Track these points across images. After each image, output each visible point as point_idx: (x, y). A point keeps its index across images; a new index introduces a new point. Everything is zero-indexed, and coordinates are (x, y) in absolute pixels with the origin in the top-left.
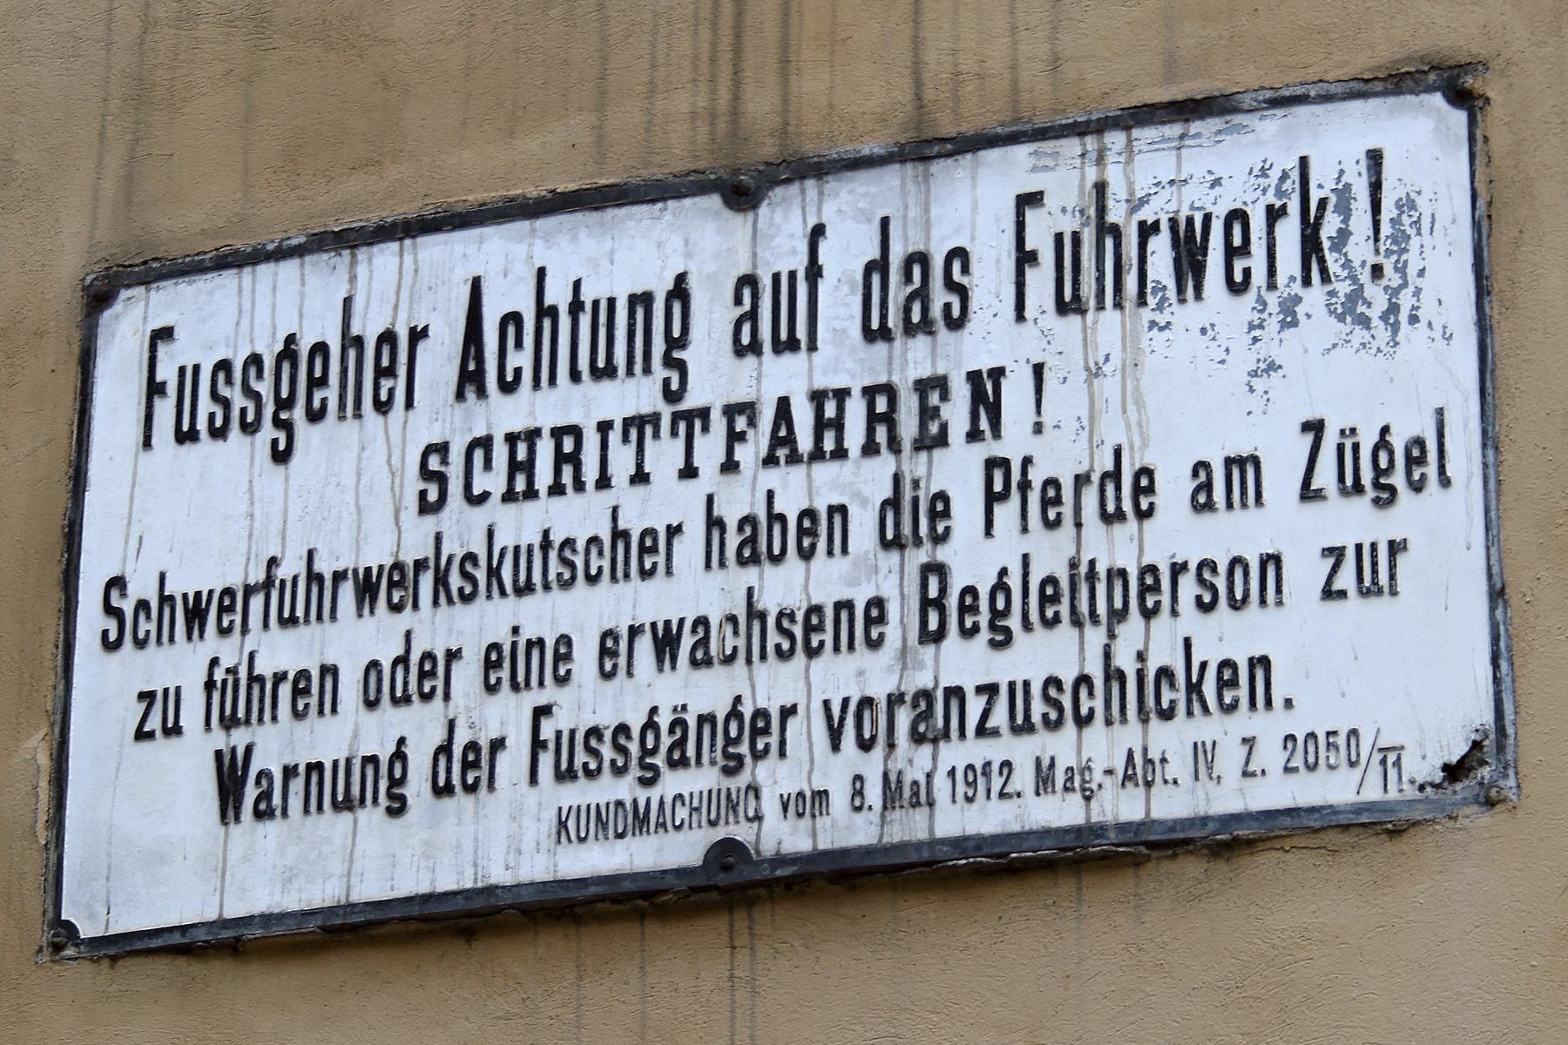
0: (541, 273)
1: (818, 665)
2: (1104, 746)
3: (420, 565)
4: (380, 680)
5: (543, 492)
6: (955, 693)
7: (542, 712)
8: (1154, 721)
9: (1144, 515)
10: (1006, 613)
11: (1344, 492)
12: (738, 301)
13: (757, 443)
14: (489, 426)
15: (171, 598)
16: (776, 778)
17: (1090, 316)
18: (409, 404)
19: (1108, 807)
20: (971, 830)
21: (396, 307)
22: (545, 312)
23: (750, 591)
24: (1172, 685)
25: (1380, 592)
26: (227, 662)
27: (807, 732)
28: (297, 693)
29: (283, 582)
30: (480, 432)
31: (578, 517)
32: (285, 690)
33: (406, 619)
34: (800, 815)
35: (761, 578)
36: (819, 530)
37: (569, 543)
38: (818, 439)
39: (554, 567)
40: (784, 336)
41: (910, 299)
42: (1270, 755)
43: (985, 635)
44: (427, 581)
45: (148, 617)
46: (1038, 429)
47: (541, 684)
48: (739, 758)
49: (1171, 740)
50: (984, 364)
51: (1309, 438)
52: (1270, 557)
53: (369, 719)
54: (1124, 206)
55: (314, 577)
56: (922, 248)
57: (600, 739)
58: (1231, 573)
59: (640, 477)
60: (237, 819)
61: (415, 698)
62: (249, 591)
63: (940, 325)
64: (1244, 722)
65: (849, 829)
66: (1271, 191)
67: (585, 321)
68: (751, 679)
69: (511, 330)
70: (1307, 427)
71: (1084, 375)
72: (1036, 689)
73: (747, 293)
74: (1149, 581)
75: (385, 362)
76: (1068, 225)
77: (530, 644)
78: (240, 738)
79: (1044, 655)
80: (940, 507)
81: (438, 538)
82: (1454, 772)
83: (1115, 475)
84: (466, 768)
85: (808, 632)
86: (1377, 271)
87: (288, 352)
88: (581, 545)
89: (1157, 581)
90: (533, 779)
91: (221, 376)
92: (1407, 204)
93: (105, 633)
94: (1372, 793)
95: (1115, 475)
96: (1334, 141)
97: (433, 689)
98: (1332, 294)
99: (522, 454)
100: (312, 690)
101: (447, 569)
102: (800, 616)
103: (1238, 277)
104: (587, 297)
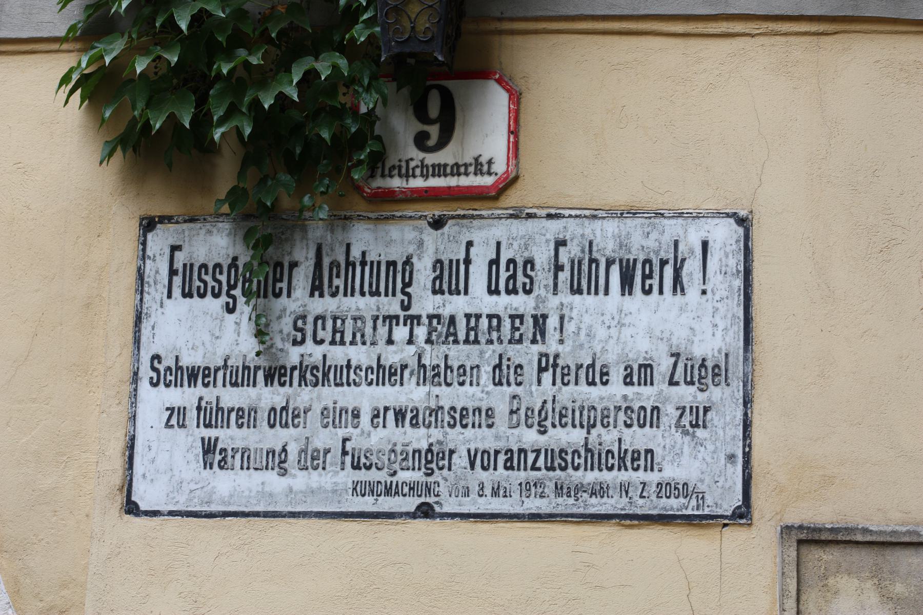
0: (348, 246)
3: (294, 368)
10: (546, 419)
12: (434, 271)
15: (181, 368)
22: (348, 263)
24: (613, 457)
28: (239, 417)
32: (233, 416)
37: (359, 367)
39: (352, 376)
40: (453, 287)
43: (536, 427)
44: (296, 373)
45: (171, 375)
62: (217, 370)
64: (641, 475)
67: (367, 269)
78: (212, 433)
83: (593, 365)
84: (313, 459)
85: (461, 417)
93: (151, 378)
95: (593, 365)
100: (245, 417)
103: (647, 287)
104: (368, 259)
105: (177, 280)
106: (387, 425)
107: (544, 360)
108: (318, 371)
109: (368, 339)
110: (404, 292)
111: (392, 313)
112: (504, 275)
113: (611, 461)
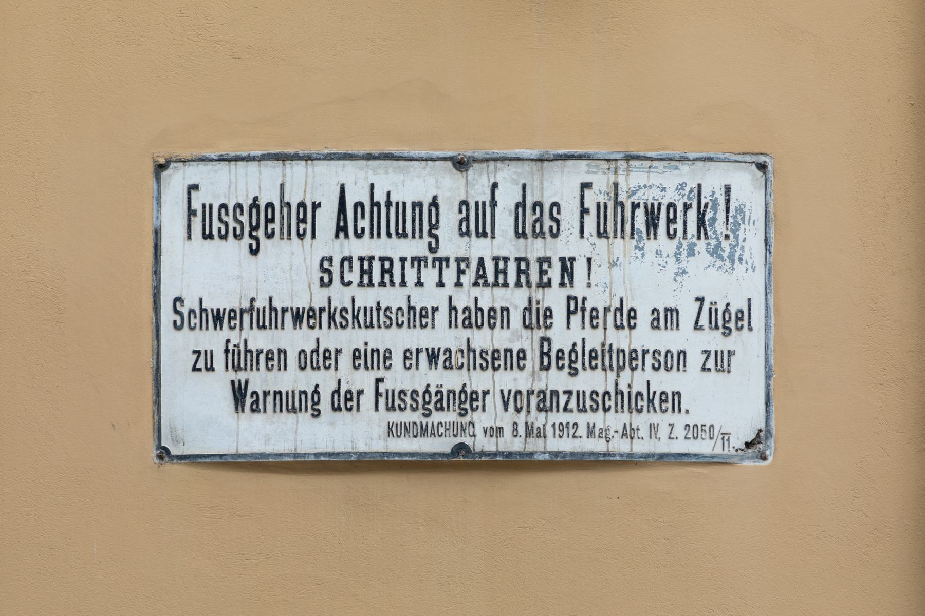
0: (372, 186)
1: (497, 374)
2: (615, 421)
3: (321, 310)
4: (306, 358)
5: (376, 285)
6: (555, 393)
7: (379, 380)
8: (634, 412)
9: (632, 328)
10: (575, 362)
11: (711, 328)
12: (460, 212)
13: (470, 276)
14: (350, 251)
15: (206, 310)
16: (482, 420)
17: (611, 240)
18: (313, 236)
19: (616, 445)
20: (561, 449)
21: (305, 191)
22: (374, 204)
23: (468, 339)
24: (642, 399)
25: (724, 371)
26: (234, 341)
27: (494, 402)
28: (268, 359)
29: (258, 309)
30: (347, 254)
31: (393, 298)
32: (262, 357)
33: (316, 333)
34: (491, 436)
35: (473, 334)
36: (496, 317)
37: (387, 309)
38: (496, 277)
39: (383, 318)
40: (481, 230)
41: (536, 221)
42: (679, 431)
43: (567, 370)
44: (325, 316)
46: (589, 285)
47: (379, 368)
48: (466, 410)
49: (641, 421)
50: (567, 255)
51: (699, 303)
52: (682, 351)
53: (302, 374)
54: (625, 195)
55: (272, 308)
56: (540, 200)
57: (405, 395)
58: (666, 356)
59: (419, 284)
60: (243, 411)
61: (322, 367)
63: (548, 235)
64: (669, 417)
65: (512, 444)
66: (685, 197)
67: (393, 210)
68: (469, 377)
69: (359, 210)
70: (697, 299)
71: (608, 265)
72: (588, 395)
73: (464, 208)
74: (634, 355)
75: (301, 216)
76: (602, 199)
77: (373, 350)
78: (242, 376)
79: (591, 381)
80: (548, 314)
81: (330, 299)
82: (748, 445)
83: (621, 309)
84: (346, 401)
85: (493, 360)
86: (727, 237)
87: (255, 204)
88: (394, 310)
89: (637, 356)
90: (377, 409)
91: (223, 211)
92: (740, 210)
93: (175, 322)
94: (718, 450)
96: (712, 180)
97: (330, 365)
98: (709, 244)
99: (366, 267)
100: (275, 359)
101: (334, 314)
102: (490, 353)
103: (672, 232)
104: (393, 199)
105: (197, 222)
106: (420, 367)
107: (572, 303)
108: (347, 312)
109: (397, 279)
110: (431, 234)
111: (421, 254)
112: (530, 219)
113: (640, 403)
